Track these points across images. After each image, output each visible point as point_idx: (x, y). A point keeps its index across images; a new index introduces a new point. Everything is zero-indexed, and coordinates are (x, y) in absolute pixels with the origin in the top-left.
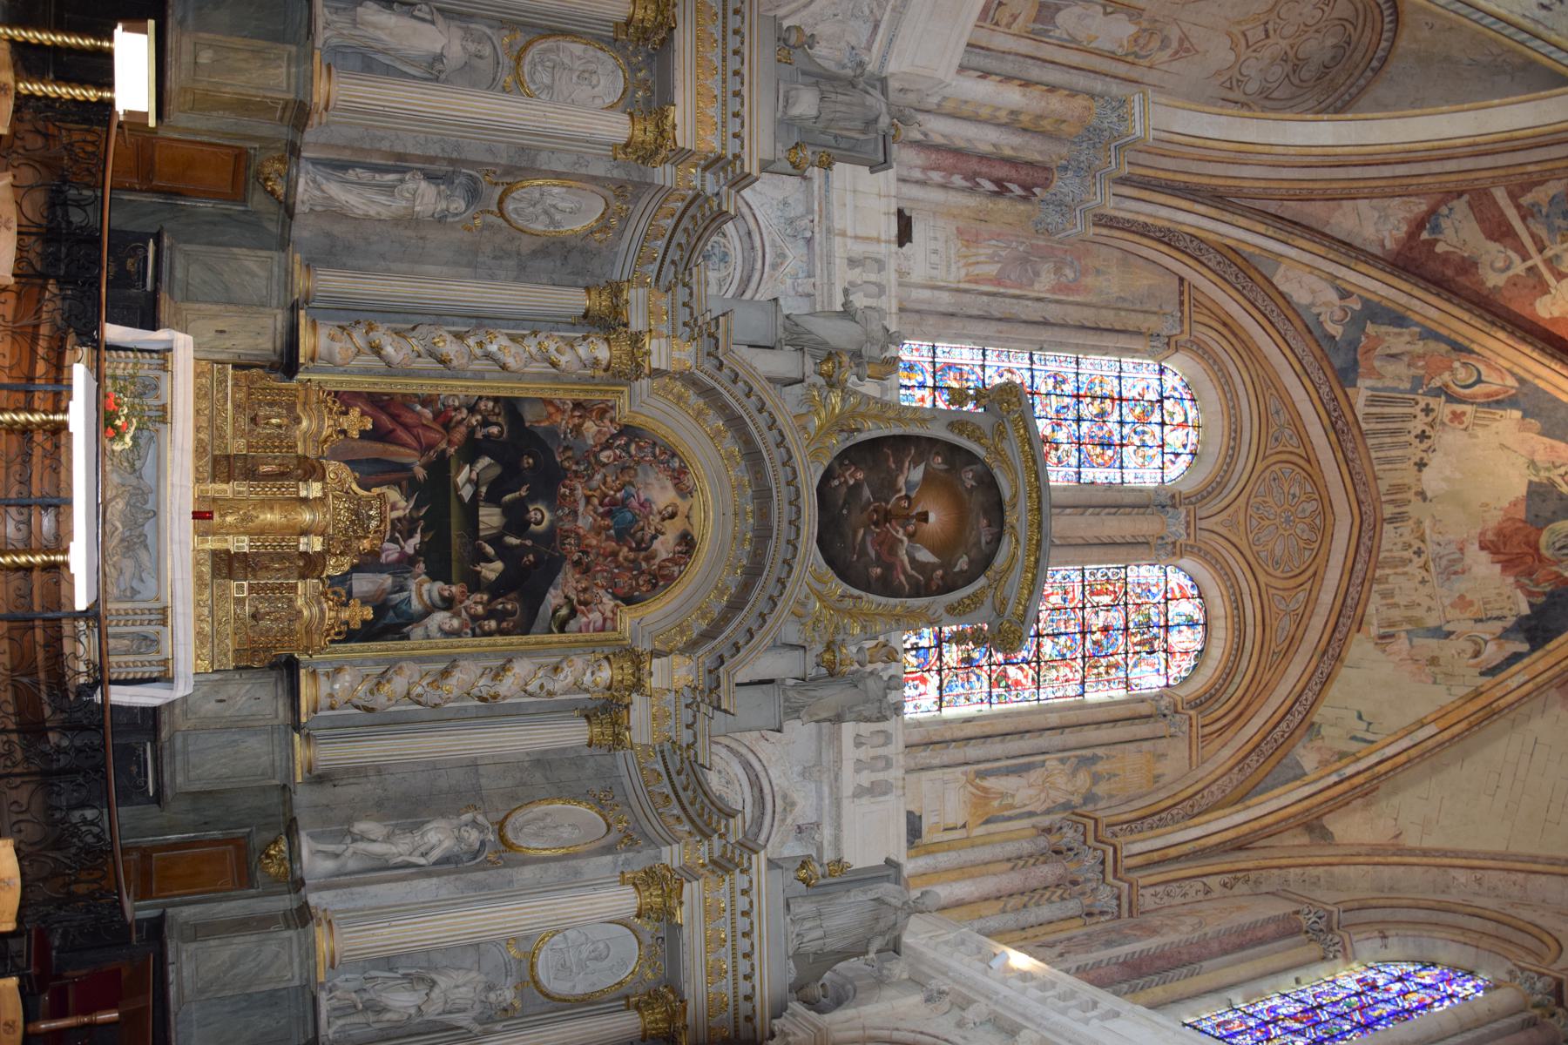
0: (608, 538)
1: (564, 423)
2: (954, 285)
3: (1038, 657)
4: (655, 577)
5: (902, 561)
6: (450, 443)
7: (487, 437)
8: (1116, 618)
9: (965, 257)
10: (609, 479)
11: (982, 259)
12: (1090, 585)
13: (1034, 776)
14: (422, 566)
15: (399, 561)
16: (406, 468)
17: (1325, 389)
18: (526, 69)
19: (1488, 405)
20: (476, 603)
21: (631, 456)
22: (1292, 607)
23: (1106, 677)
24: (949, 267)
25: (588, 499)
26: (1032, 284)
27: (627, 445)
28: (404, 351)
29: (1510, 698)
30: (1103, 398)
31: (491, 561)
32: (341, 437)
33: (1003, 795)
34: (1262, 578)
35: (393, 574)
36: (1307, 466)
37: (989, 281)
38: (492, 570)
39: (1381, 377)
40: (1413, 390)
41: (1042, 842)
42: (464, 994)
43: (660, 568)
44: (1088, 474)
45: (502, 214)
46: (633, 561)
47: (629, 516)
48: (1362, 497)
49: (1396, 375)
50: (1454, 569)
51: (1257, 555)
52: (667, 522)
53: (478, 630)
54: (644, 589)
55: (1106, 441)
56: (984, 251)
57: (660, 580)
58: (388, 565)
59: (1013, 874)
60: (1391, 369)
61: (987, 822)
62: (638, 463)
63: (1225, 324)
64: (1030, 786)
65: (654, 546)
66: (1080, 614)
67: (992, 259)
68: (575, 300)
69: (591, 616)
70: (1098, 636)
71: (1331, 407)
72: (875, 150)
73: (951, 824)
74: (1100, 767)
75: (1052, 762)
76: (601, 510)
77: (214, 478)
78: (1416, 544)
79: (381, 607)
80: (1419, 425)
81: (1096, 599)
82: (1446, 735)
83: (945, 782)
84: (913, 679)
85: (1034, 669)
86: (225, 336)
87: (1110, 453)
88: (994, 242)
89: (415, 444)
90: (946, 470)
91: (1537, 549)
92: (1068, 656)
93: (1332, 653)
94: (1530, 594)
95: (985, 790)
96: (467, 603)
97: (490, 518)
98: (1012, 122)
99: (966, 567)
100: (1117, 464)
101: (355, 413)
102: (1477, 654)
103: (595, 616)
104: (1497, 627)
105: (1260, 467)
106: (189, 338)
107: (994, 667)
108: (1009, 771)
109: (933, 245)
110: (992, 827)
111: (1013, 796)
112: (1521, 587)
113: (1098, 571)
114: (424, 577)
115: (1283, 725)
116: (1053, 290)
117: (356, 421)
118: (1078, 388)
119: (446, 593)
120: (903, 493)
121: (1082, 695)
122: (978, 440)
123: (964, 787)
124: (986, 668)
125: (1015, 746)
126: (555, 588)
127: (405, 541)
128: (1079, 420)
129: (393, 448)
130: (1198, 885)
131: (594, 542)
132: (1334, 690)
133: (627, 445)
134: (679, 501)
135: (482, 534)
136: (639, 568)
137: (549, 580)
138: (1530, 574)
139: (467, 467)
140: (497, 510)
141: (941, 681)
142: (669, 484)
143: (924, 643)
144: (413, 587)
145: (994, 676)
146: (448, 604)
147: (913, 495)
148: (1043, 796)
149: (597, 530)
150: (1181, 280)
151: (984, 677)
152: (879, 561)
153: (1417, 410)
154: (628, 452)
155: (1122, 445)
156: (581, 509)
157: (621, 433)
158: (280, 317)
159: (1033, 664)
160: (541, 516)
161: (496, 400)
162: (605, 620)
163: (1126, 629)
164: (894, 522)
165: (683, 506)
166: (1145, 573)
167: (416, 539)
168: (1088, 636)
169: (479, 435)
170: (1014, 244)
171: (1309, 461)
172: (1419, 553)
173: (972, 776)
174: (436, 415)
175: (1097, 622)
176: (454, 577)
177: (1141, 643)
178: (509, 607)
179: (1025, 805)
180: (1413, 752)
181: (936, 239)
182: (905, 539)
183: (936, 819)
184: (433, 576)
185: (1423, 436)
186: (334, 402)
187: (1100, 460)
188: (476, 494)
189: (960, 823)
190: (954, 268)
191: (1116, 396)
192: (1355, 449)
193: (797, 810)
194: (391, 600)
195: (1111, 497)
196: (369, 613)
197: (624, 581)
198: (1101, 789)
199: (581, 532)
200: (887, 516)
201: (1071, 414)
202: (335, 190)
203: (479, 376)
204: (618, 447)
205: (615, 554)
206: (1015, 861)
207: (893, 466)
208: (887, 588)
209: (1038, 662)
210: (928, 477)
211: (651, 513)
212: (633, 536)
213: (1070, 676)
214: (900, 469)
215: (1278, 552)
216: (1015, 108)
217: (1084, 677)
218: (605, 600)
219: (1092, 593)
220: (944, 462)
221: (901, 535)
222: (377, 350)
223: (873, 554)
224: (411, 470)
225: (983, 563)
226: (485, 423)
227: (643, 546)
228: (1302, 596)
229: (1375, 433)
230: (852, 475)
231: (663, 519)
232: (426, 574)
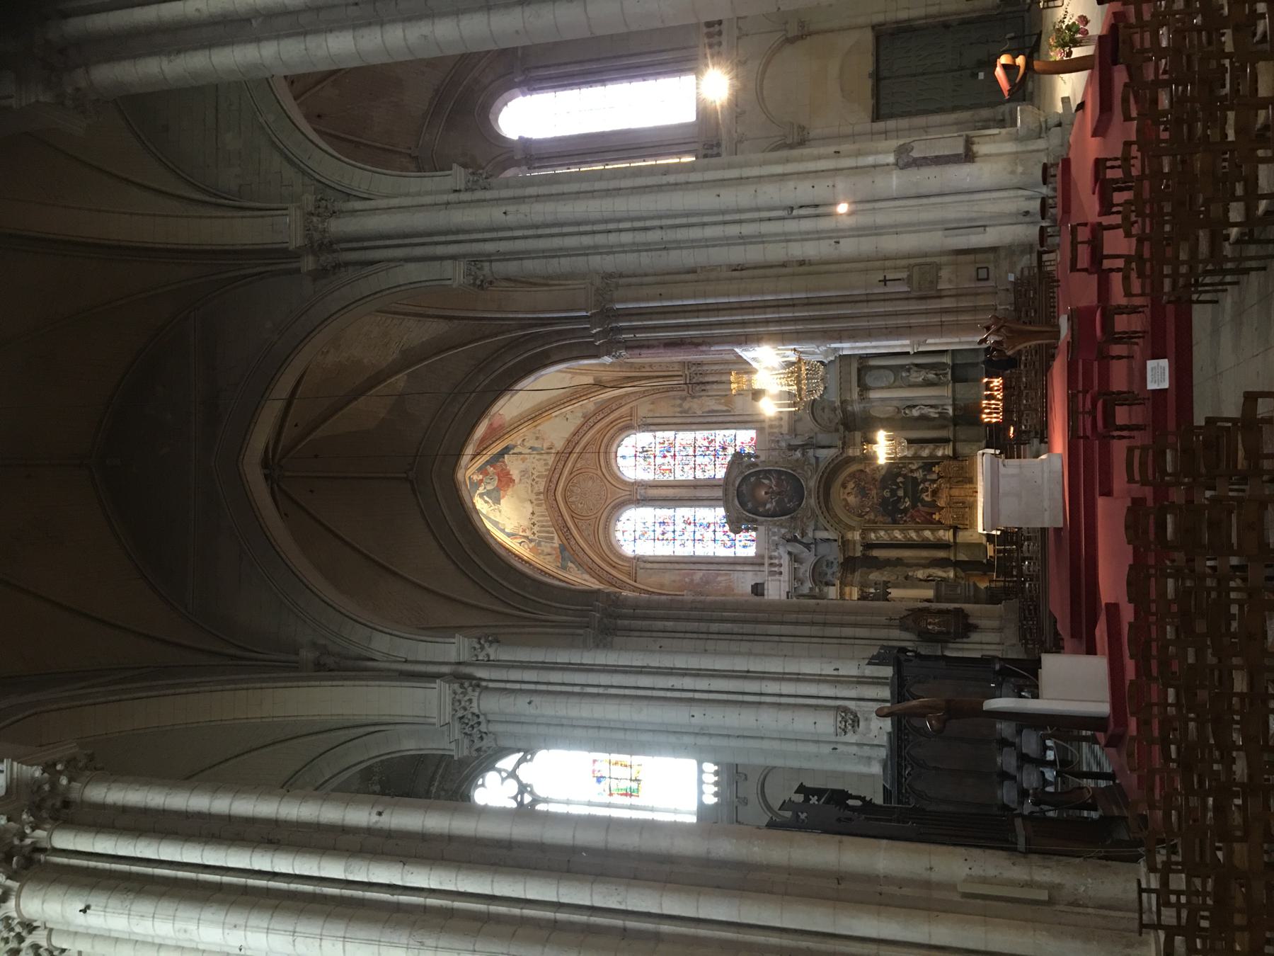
1: (880, 518)
8: (659, 460)
13: (707, 409)
16: (923, 506)
17: (573, 542)
19: (516, 535)
22: (583, 462)
26: (704, 575)
29: (527, 424)
33: (720, 404)
34: (599, 472)
36: (574, 515)
39: (552, 547)
40: (540, 542)
42: (914, 375)
48: (554, 502)
49: (546, 548)
50: (524, 473)
51: (602, 480)
56: (723, 584)
57: (852, 475)
60: (548, 550)
63: (614, 567)
66: (677, 462)
67: (720, 582)
68: (876, 553)
71: (570, 536)
74: (679, 409)
78: (534, 483)
79: (930, 471)
80: (536, 529)
81: (669, 467)
82: (550, 412)
91: (499, 480)
92: (682, 448)
93: (571, 443)
94: (504, 462)
101: (937, 519)
102: (524, 440)
104: (515, 450)
105: (599, 514)
108: (717, 411)
110: (724, 393)
112: (506, 465)
113: (668, 477)
115: (599, 418)
117: (936, 517)
125: (714, 419)
128: (674, 532)
130: (655, 369)
132: (572, 429)
138: (502, 470)
146: (912, 471)
149: (870, 490)
150: (635, 581)
151: (717, 444)
152: (782, 480)
153: (537, 534)
160: (886, 494)
163: (655, 457)
165: (845, 496)
166: (648, 476)
171: (573, 517)
172: (534, 480)
175: (669, 459)
177: (647, 451)
180: (562, 406)
184: (916, 478)
185: (534, 524)
192: (557, 521)
196: (933, 469)
198: (678, 402)
200: (779, 493)
202: (944, 575)
208: (779, 472)
210: (765, 505)
215: (590, 483)
221: (775, 488)
225: (745, 479)
227: (857, 485)
228: (578, 465)
229: (549, 527)
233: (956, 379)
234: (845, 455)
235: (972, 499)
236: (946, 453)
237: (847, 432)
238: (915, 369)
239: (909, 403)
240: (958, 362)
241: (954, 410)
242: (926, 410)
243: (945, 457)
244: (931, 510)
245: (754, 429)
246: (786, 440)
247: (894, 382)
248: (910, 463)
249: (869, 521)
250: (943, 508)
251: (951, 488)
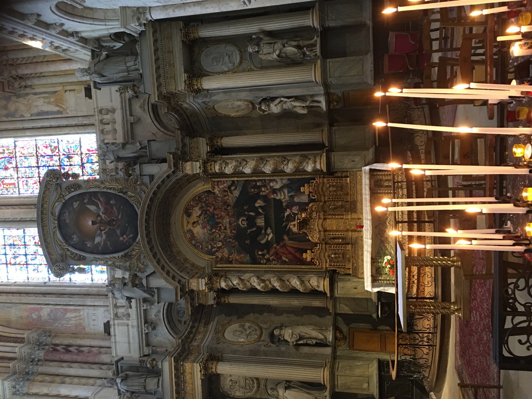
0: (217, 215)
1: (235, 256)
2: (85, 307)
3: (37, 158)
4: (200, 200)
5: (102, 206)
6: (276, 248)
7: (262, 251)
9: (81, 319)
10: (218, 236)
11: (74, 319)
12: (15, 187)
13: (35, 111)
14: (284, 205)
15: (292, 206)
16: (290, 239)
18: (255, 385)
20: (264, 191)
21: (210, 244)
23: (4, 149)
24: (88, 315)
25: (225, 229)
26: (51, 311)
27: (212, 248)
28: (293, 282)
30: (15, 264)
31: (259, 206)
32: (313, 251)
33: (49, 103)
35: (294, 202)
37: (71, 311)
38: (259, 203)
41: (29, 83)
42: (266, 49)
43: (198, 204)
44: (20, 232)
45: (261, 328)
46: (208, 206)
47: (210, 223)
52: (196, 220)
53: (264, 181)
54: (203, 196)
55: (12, 246)
56: (73, 322)
57: (198, 199)
59: (42, 71)
61: (56, 92)
62: (208, 242)
64: (37, 106)
65: (201, 212)
67: (70, 319)
68: (233, 300)
69: (223, 186)
70: (10, 166)
72: (121, 367)
73: (72, 94)
75: (27, 116)
76: (221, 225)
77: (357, 238)
81: (12, 181)
83: (76, 110)
84: (93, 151)
85: (39, 153)
86: (354, 287)
87: (11, 242)
88: (69, 326)
89: (288, 247)
90: (85, 241)
92: (23, 158)
95: (58, 106)
96: (267, 192)
97: (260, 222)
98: (63, 378)
99: (74, 203)
100: (6, 237)
101: (309, 259)
106: (366, 289)
107: (58, 154)
108: (47, 113)
109: (95, 323)
110: (53, 89)
111: (44, 102)
114: (283, 201)
116: (41, 309)
117: (308, 256)
118: (27, 268)
119: (275, 195)
120: (103, 232)
121: (15, 141)
122: (72, 253)
123: (67, 108)
124: (61, 154)
126: (236, 196)
127: (290, 213)
129: (295, 246)
131: (222, 213)
133: (212, 248)
134: (192, 228)
135: (263, 216)
136: (206, 204)
137: (238, 199)
139: (269, 239)
140: (258, 224)
141: (80, 149)
142: (196, 234)
143: (89, 165)
144: (287, 197)
145: (57, 151)
146: (274, 191)
147: (99, 232)
148: (30, 102)
149: (222, 218)
151: (61, 150)
154: (211, 246)
155: (5, 245)
156: (228, 225)
157: (215, 252)
158: (336, 294)
159: (39, 155)
160: (242, 222)
161: (260, 264)
162: (218, 185)
164: (106, 221)
165: (190, 226)
167: (286, 214)
168: (15, 166)
169: (265, 251)
170: (60, 326)
173: (64, 112)
174: (281, 258)
175: (11, 172)
176: (272, 201)
178: (252, 190)
179: (38, 98)
181: (94, 325)
182: (101, 214)
183: (78, 95)
186: (316, 263)
187: (15, 239)
188: (266, 230)
189: (68, 92)
190: (86, 315)
191: (9, 265)
193: (139, 104)
194: (295, 193)
195: (8, 225)
197: (211, 199)
199: (227, 217)
200: (109, 223)
201: (29, 257)
203: (266, 272)
204: (215, 248)
205: (215, 209)
206: (41, 76)
207: (108, 242)
208: (108, 196)
209: (37, 156)
211: (202, 224)
212: (208, 216)
213: (22, 150)
214: (105, 241)
216: (63, 385)
217: (15, 149)
218: (218, 192)
219: (14, 184)
220: (86, 244)
221: (103, 216)
222: (302, 282)
223: (114, 208)
224: (289, 238)
225: (66, 205)
226: (263, 255)
227: (204, 212)
230: (125, 238)
231: (197, 222)
232: (282, 202)
233: (326, 54)
234: (180, 174)
235: (355, 235)
236: (318, 167)
237: (187, 140)
238: (266, 39)
239: (264, 95)
240: (331, 24)
241: (329, 102)
242: (289, 104)
243: (316, 172)
244: (301, 246)
245: (94, 133)
246: (113, 151)
247: (241, 62)
248: (271, 181)
249: (222, 260)
250: (316, 244)
251: (325, 219)
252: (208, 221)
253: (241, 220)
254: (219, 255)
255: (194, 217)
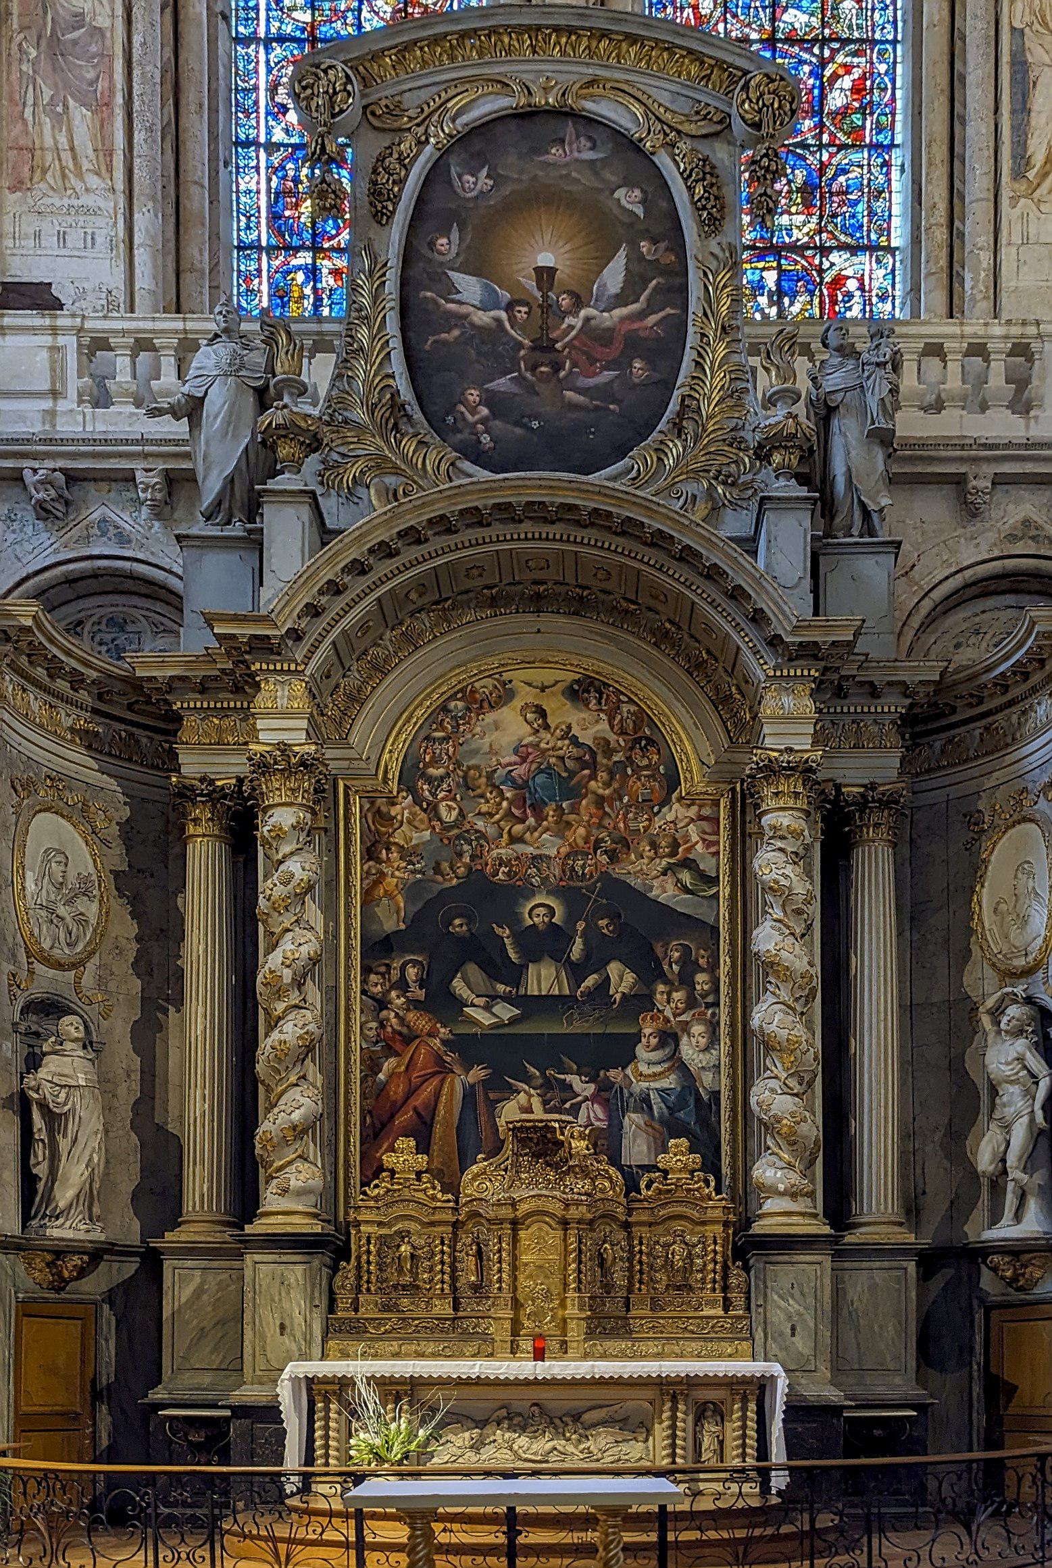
0: (575, 810)
1: (396, 873)
4: (637, 741)
6: (431, 1034)
10: (484, 808)
14: (612, 1073)
15: (605, 1104)
16: (469, 1094)
21: (448, 775)
25: (514, 840)
27: (430, 780)
31: (608, 979)
43: (623, 732)
53: (710, 999)
54: (656, 757)
58: (610, 1118)
62: (458, 764)
69: (695, 838)
76: (531, 821)
89: (435, 1081)
96: (668, 1013)
103: (693, 832)
114: (629, 1071)
119: (654, 1041)
126: (651, 888)
131: (581, 831)
133: (430, 780)
134: (518, 703)
137: (640, 898)
142: (490, 717)
146: (669, 1038)
149: (563, 827)
154: (442, 779)
156: (530, 850)
157: (413, 790)
161: (366, 970)
167: (575, 1081)
169: (421, 994)
178: (677, 954)
188: (506, 998)
197: (640, 787)
199: (564, 850)
203: (331, 994)
204: (434, 795)
205: (600, 801)
212: (572, 774)
218: (670, 817)
224: (472, 1086)
226: (402, 985)
227: (589, 759)
231: (547, 727)
252: (549, 771)
253: (550, 902)
254: (403, 808)
255: (564, 713)
